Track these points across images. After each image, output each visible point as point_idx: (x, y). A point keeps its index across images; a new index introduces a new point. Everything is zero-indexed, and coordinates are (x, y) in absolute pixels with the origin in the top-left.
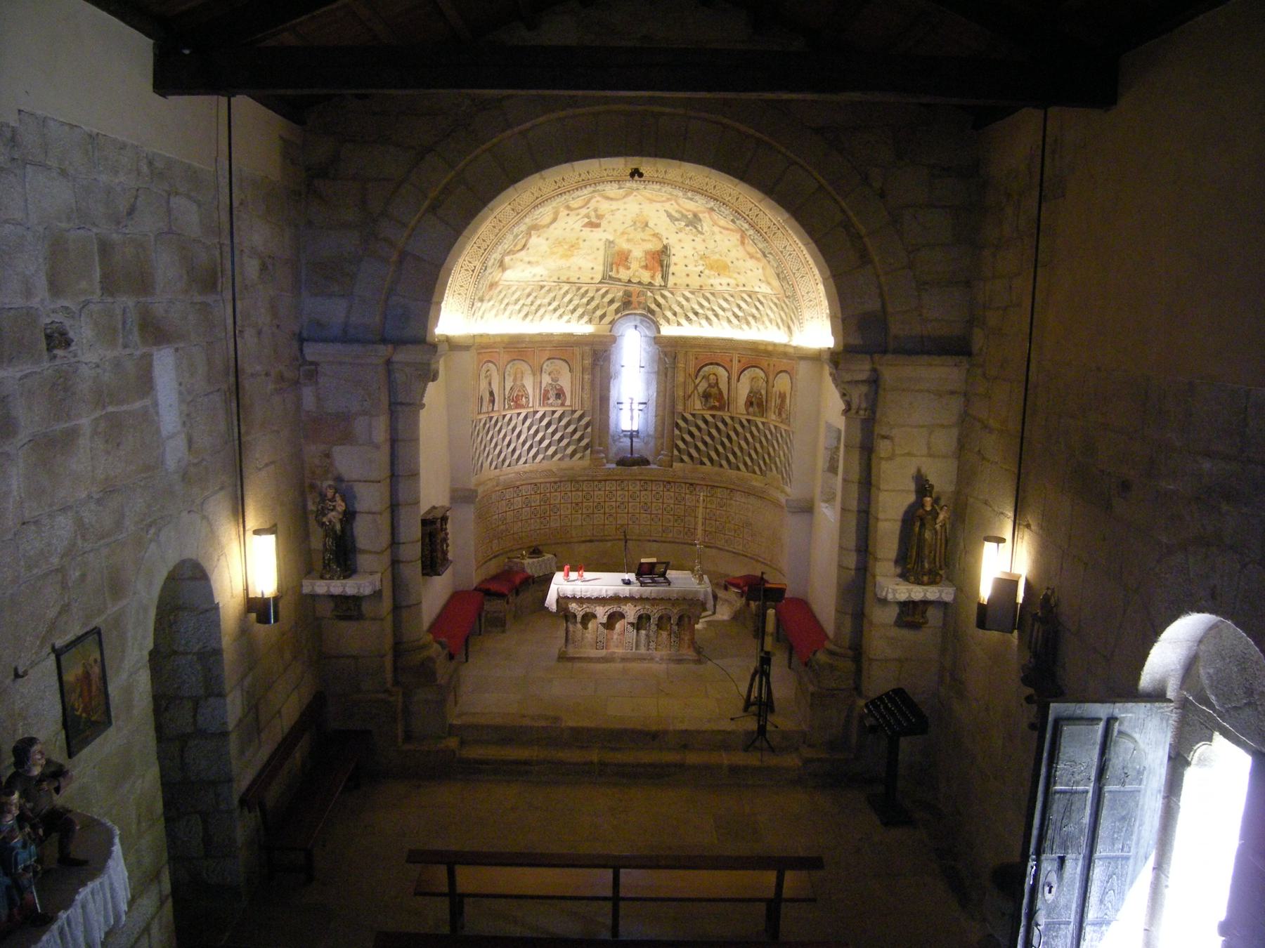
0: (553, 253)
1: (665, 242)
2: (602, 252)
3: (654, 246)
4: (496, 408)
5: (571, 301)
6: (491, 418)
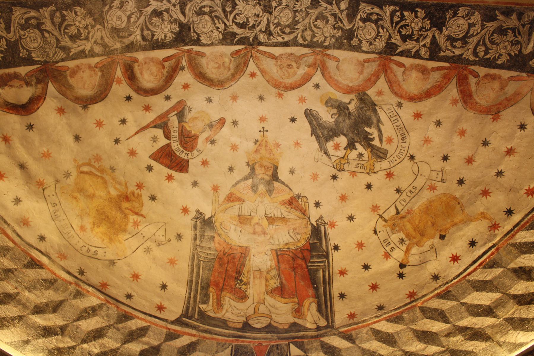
0: (81, 190)
1: (314, 214)
2: (185, 248)
3: (289, 235)
5: (97, 334)
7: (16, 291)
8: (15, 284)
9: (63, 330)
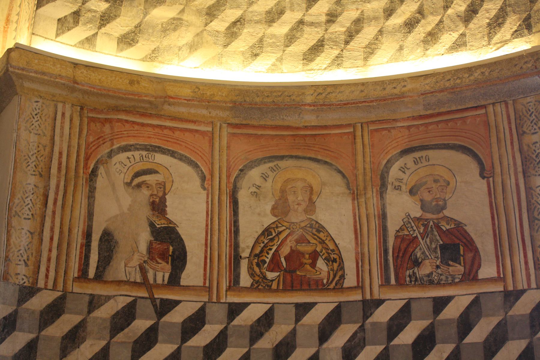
4: (192, 274)
6: (165, 307)
7: (359, 12)
8: (354, 7)
9: (420, 11)
